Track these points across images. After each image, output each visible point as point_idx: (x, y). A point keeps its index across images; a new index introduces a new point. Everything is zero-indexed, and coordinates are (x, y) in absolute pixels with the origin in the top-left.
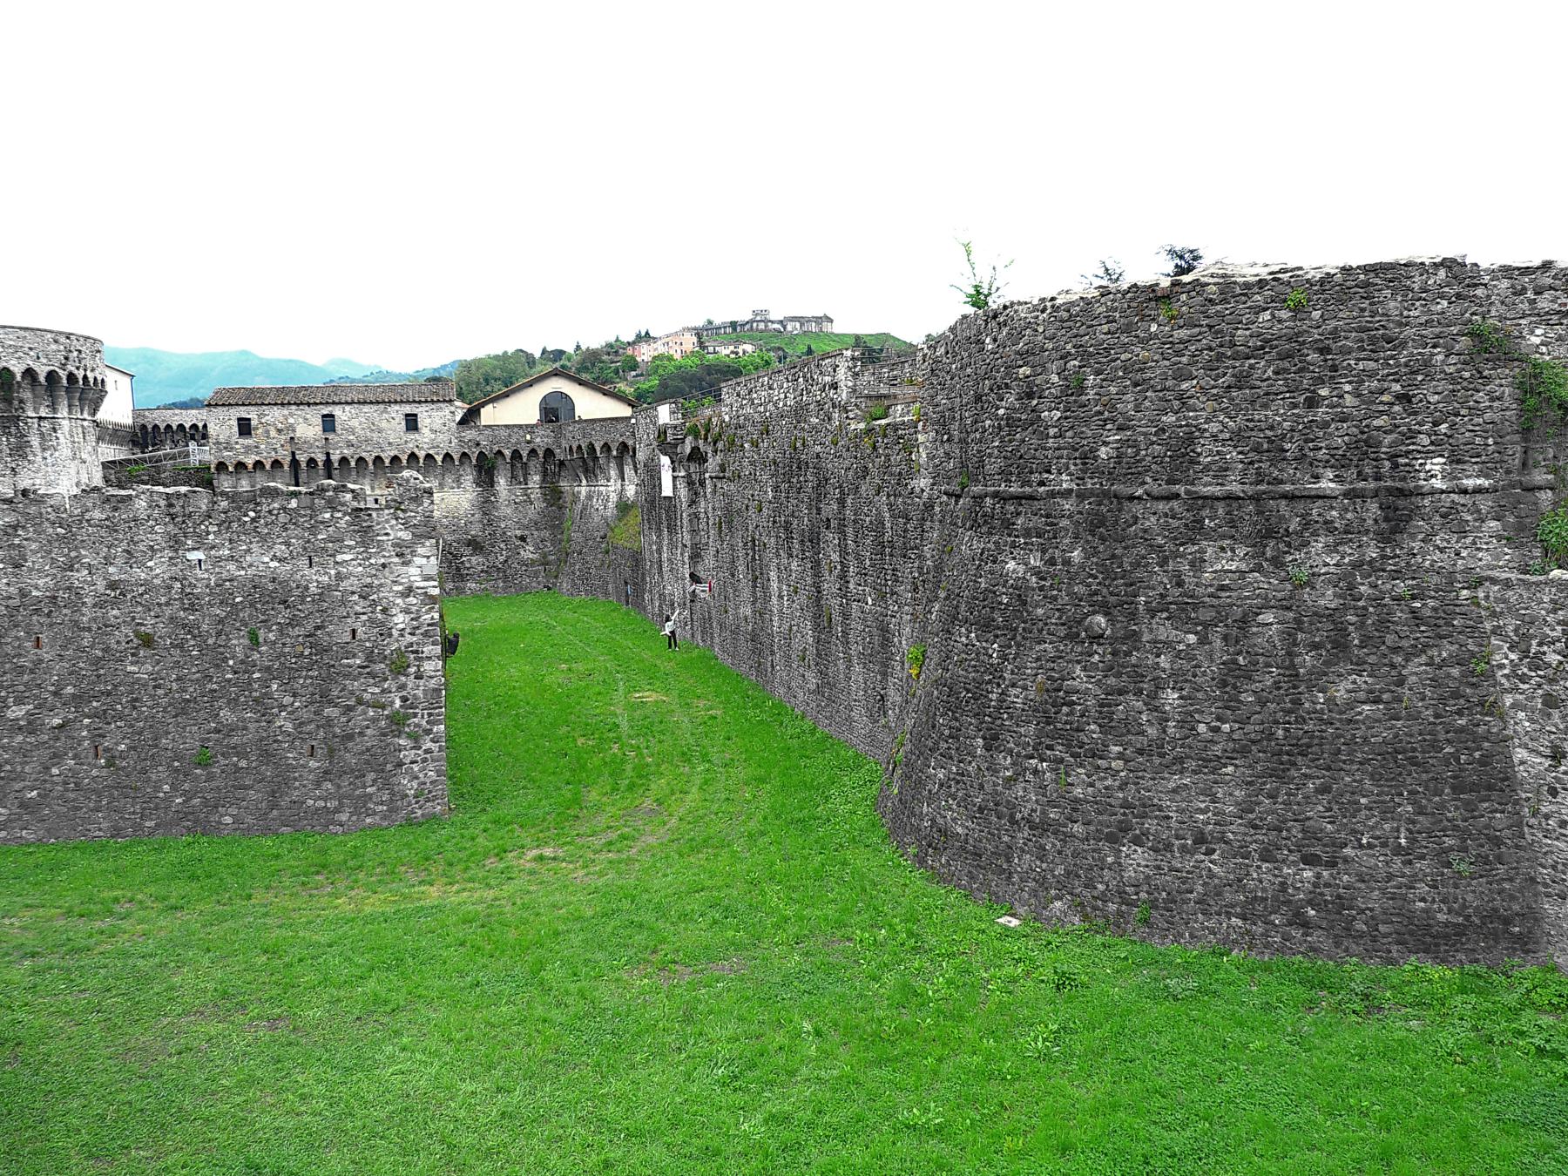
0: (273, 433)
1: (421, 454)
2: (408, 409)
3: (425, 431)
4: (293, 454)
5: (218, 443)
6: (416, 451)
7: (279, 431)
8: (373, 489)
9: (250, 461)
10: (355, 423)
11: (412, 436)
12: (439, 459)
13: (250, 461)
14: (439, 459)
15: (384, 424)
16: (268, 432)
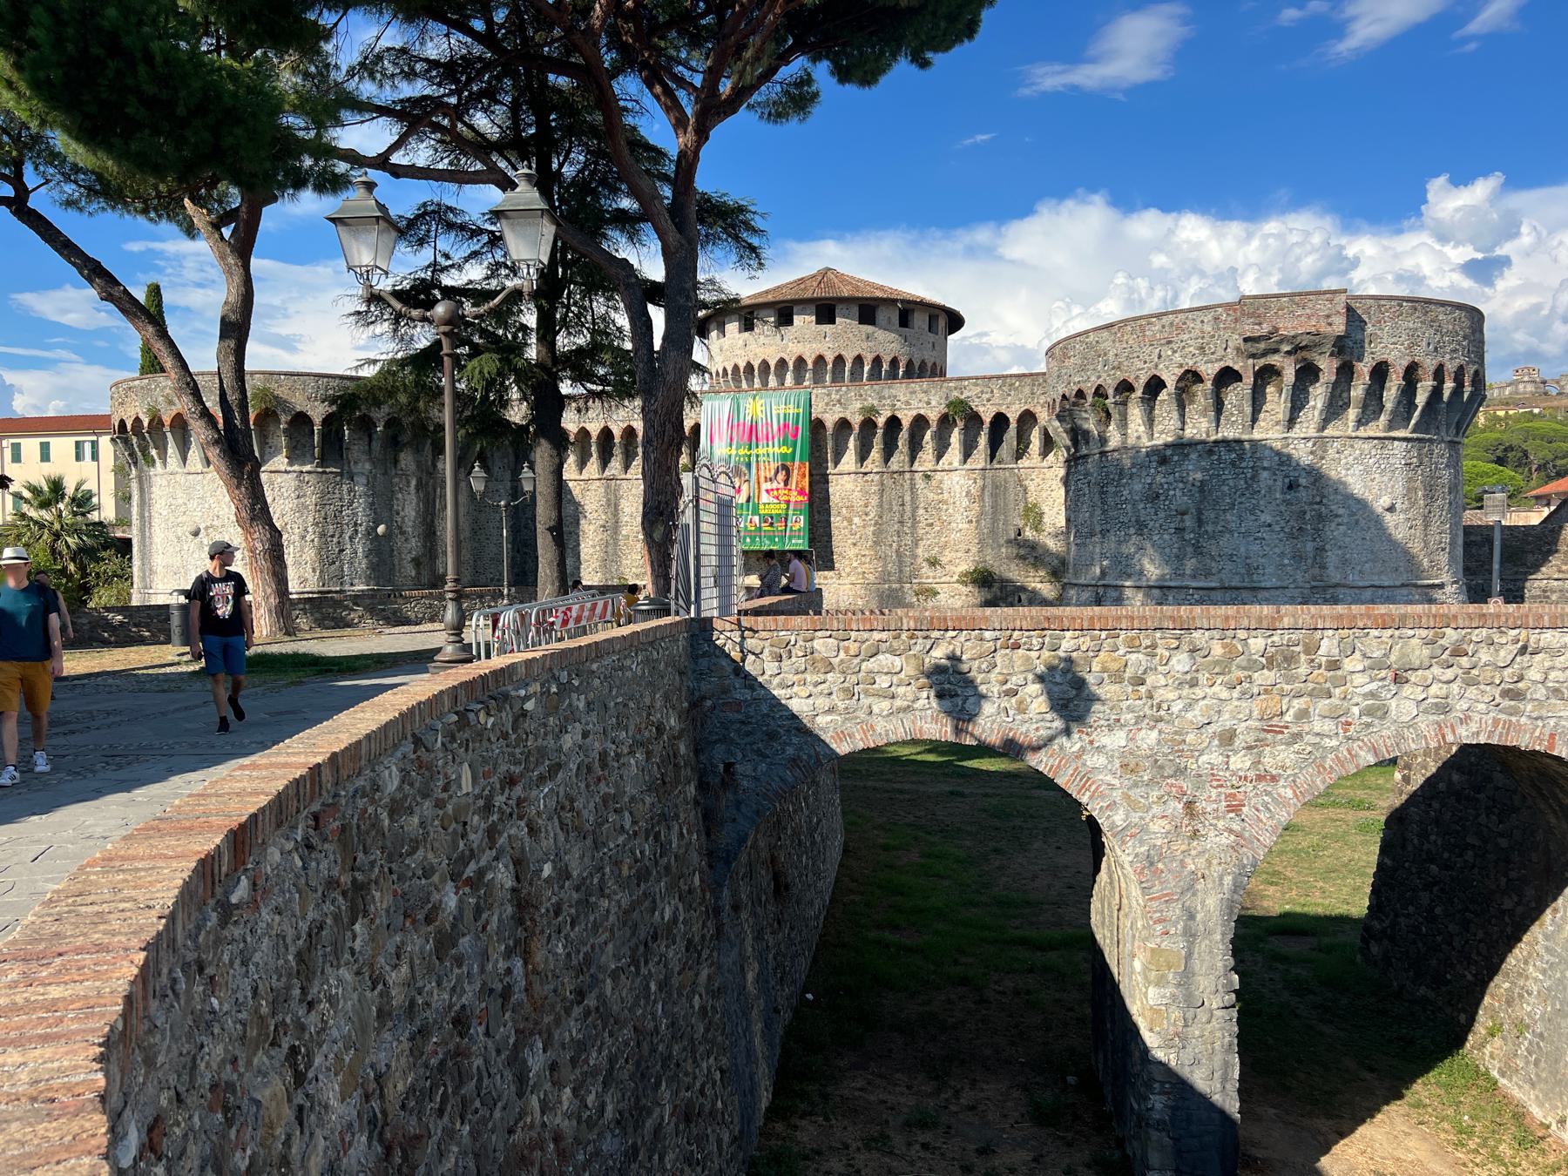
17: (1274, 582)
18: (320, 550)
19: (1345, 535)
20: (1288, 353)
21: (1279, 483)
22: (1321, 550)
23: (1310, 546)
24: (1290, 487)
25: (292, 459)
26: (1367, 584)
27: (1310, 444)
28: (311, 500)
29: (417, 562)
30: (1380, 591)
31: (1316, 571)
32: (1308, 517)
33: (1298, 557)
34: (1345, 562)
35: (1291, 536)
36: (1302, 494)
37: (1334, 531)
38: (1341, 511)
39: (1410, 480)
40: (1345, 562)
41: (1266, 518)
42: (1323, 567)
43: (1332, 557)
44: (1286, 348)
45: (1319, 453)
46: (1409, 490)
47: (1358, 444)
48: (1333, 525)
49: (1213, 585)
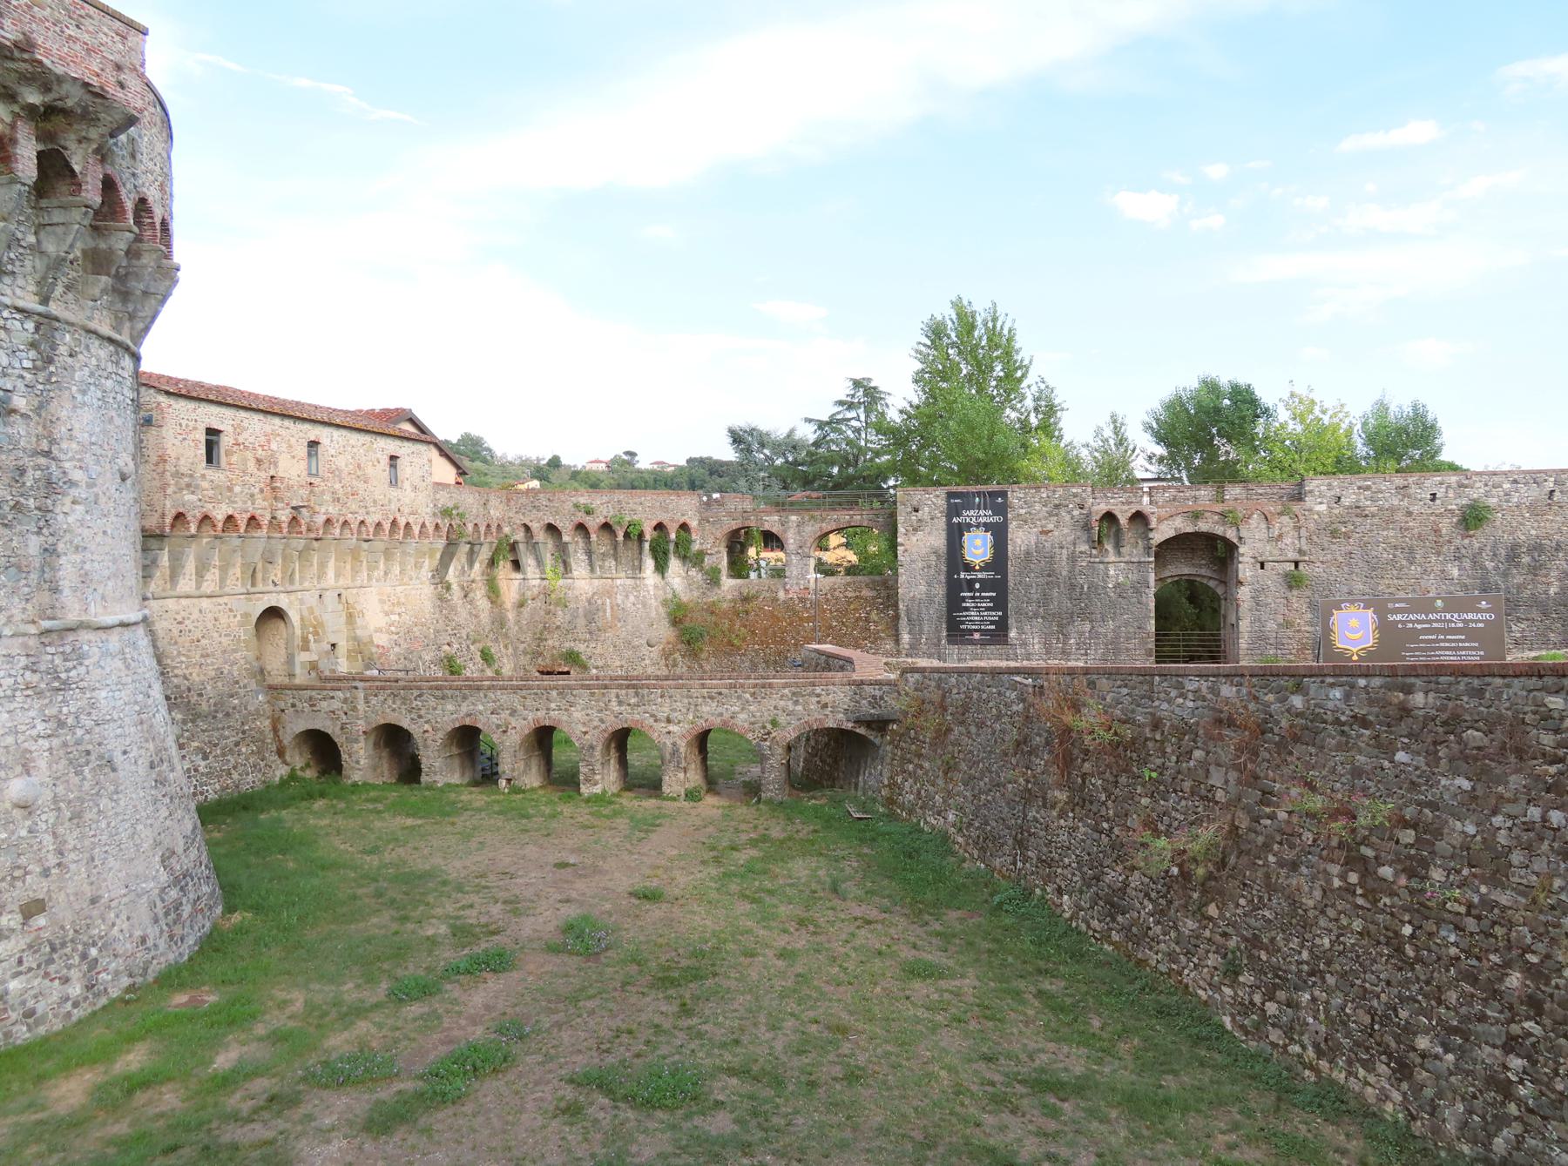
0: (251, 465)
1: (402, 522)
2: (392, 446)
3: (407, 485)
4: (273, 510)
5: (178, 475)
6: (398, 515)
7: (259, 461)
8: (338, 575)
9: (219, 516)
10: (341, 462)
11: (394, 493)
12: (416, 529)
13: (219, 516)
14: (416, 529)
15: (370, 471)
16: (245, 461)
19: (82, 522)
20: (31, 109)
22: (50, 552)
23: (34, 544)
27: (30, 326)
31: (45, 597)
34: (85, 578)
37: (68, 514)
38: (77, 475)
40: (85, 578)
42: (55, 590)
44: (33, 98)
47: (95, 344)
48: (68, 500)
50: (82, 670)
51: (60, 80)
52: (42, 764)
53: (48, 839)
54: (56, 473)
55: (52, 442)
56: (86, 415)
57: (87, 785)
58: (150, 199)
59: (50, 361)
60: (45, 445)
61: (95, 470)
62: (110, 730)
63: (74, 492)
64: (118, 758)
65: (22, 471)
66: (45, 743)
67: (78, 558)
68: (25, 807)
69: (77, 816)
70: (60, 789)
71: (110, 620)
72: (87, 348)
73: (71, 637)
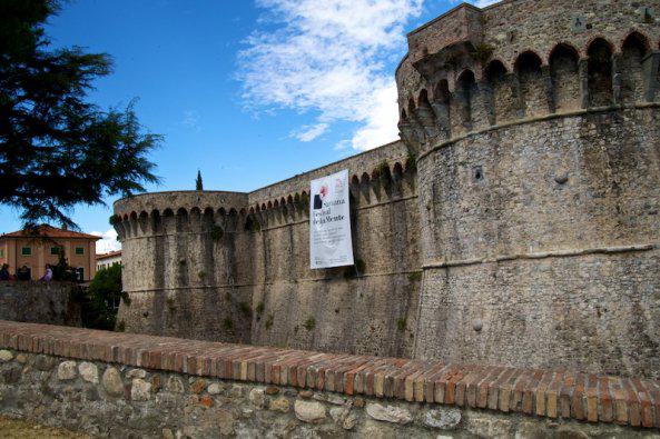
17: (475, 259)
18: (157, 269)
21: (470, 174)
23: (495, 224)
24: (478, 176)
25: (144, 231)
26: (544, 253)
28: (152, 249)
29: (202, 275)
30: (560, 260)
31: (502, 246)
32: (492, 198)
33: (488, 235)
34: (525, 236)
35: (482, 217)
36: (486, 181)
37: (514, 209)
38: (517, 190)
39: (586, 152)
40: (525, 236)
41: (465, 204)
42: (507, 242)
43: (513, 232)
45: (495, 142)
46: (587, 161)
49: (440, 263)
50: (517, 277)
51: (440, 52)
52: (488, 315)
53: (483, 345)
54: (503, 191)
55: (502, 179)
56: (521, 162)
57: (505, 328)
58: (533, 49)
59: (497, 146)
60: (497, 182)
61: (529, 184)
62: (527, 307)
63: (517, 198)
64: (529, 319)
65: (489, 196)
66: (491, 307)
67: (519, 227)
68: (478, 330)
69: (497, 340)
70: (493, 327)
71: (537, 254)
72: (521, 132)
73: (513, 262)
